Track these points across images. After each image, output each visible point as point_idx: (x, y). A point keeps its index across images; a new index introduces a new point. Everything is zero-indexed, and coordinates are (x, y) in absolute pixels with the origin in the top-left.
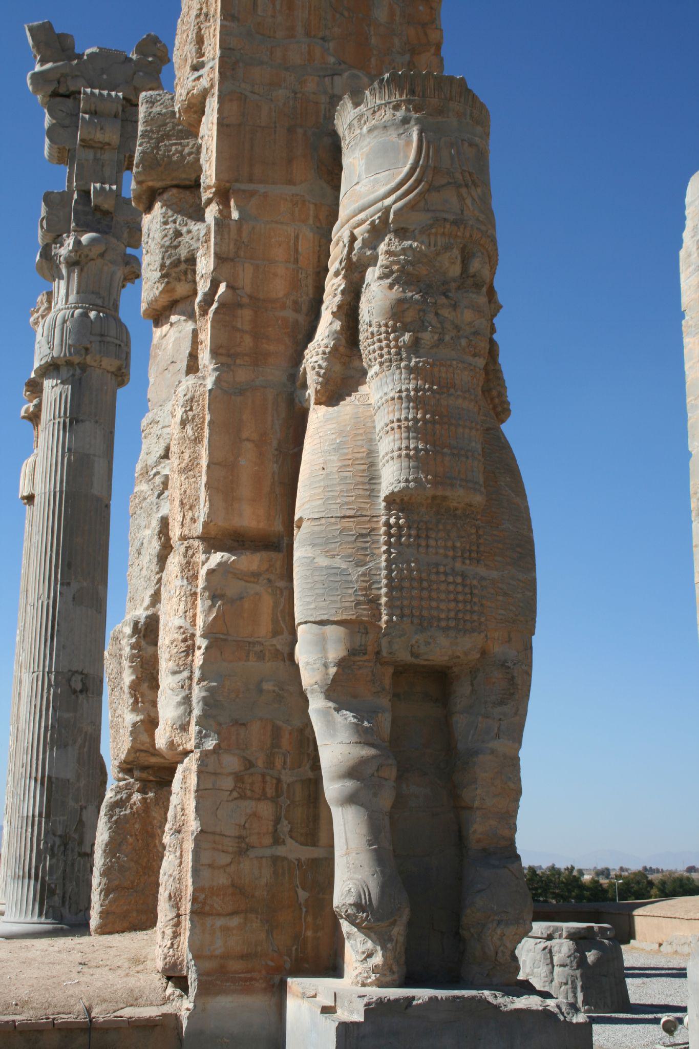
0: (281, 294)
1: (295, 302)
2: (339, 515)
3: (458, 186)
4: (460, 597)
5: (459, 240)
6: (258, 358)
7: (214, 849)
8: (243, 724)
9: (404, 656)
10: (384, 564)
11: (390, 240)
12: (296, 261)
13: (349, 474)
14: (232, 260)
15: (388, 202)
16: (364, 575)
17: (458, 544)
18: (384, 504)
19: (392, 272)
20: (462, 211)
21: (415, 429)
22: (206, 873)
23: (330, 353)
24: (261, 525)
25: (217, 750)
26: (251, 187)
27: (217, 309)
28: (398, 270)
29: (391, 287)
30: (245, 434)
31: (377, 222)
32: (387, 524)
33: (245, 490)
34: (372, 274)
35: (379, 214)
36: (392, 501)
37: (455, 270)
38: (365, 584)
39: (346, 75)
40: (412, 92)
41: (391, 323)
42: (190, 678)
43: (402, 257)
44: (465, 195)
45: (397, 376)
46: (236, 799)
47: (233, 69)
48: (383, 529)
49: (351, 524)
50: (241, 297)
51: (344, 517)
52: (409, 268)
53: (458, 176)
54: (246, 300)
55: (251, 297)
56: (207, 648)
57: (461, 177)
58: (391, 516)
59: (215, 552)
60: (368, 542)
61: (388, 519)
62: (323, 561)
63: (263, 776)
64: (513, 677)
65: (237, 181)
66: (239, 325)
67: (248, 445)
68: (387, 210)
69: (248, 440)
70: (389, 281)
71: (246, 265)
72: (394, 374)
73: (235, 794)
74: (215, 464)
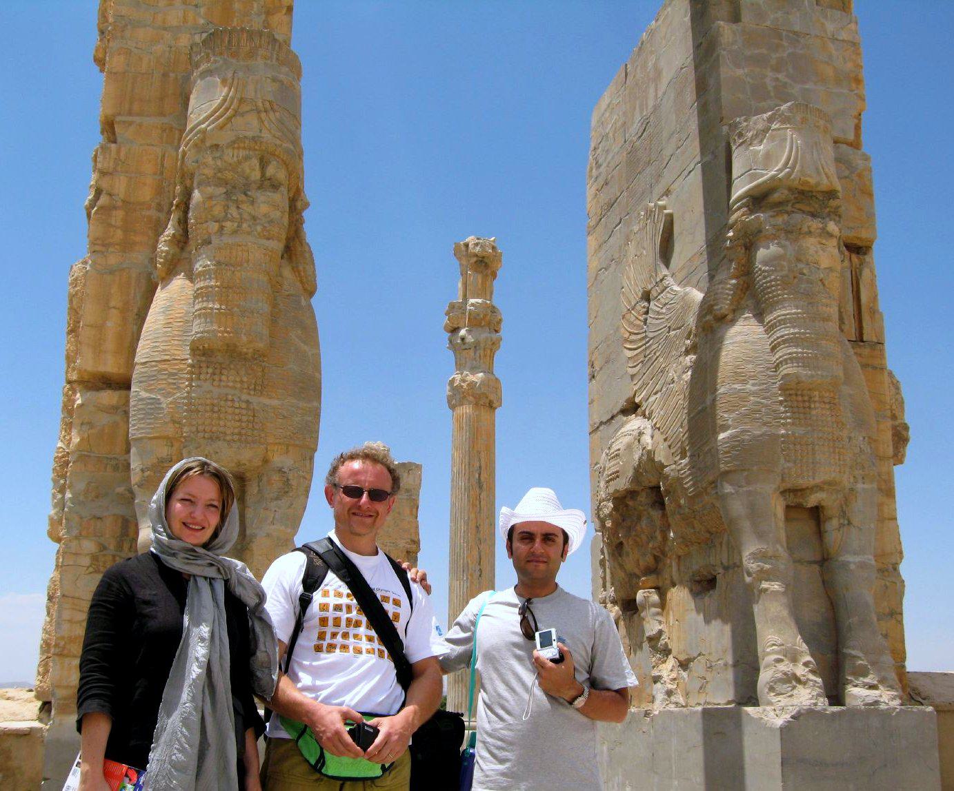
0: (148, 198)
1: (159, 204)
3: (259, 112)
4: (244, 418)
5: (257, 152)
6: (126, 246)
7: (73, 609)
8: (101, 518)
12: (162, 173)
13: (169, 329)
14: (111, 174)
17: (245, 379)
22: (66, 626)
24: (122, 371)
25: (77, 538)
26: (130, 119)
30: (112, 304)
33: (110, 345)
37: (256, 175)
44: (264, 119)
46: (91, 573)
49: (166, 366)
52: (219, 175)
53: (260, 104)
54: (119, 204)
55: (123, 201)
57: (261, 105)
63: (114, 556)
64: (288, 479)
65: (119, 114)
66: (113, 223)
67: (114, 311)
69: (114, 307)
71: (122, 178)
73: (91, 569)
74: (88, 326)
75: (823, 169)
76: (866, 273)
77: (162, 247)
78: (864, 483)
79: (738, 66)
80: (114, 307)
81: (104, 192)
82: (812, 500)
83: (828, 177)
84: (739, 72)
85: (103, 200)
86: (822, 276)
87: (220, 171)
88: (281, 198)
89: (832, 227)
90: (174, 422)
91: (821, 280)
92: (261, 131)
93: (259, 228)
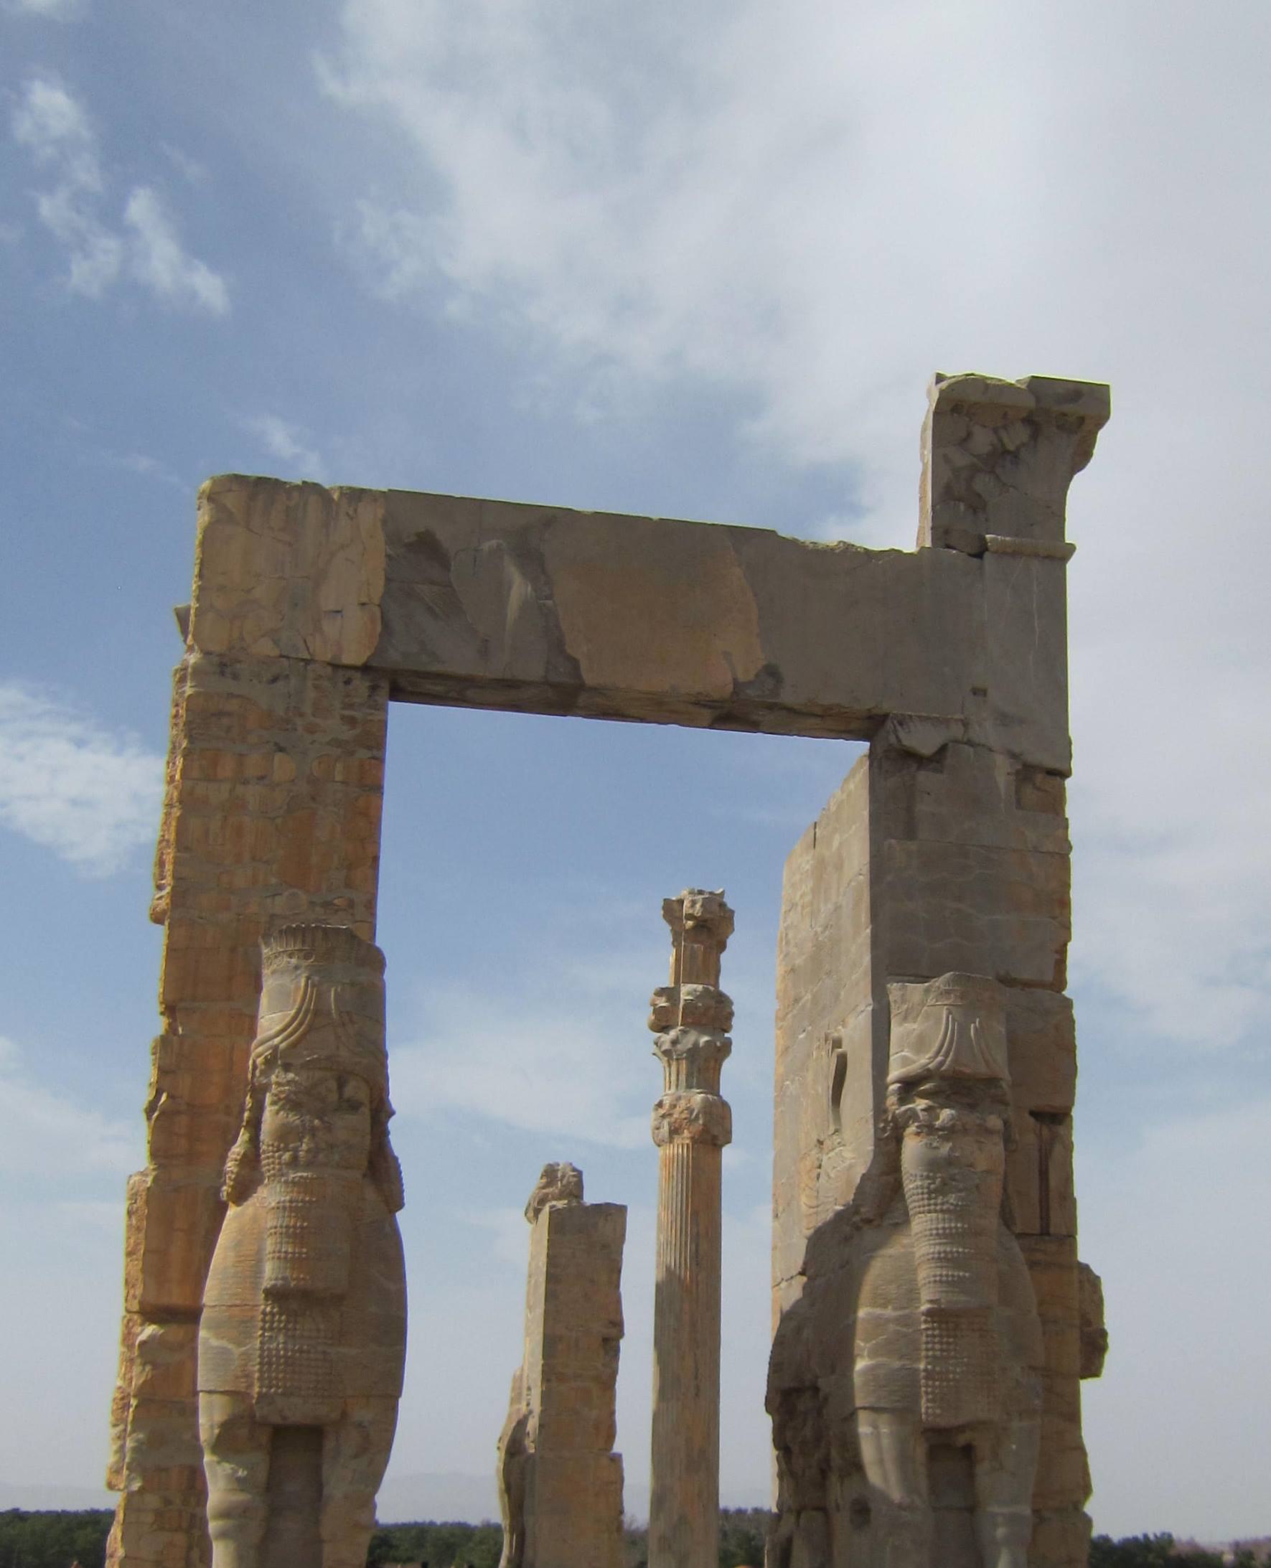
1: (228, 1107)
2: (229, 1304)
9: (276, 1419)
10: (258, 1346)
11: (279, 1072)
15: (277, 1040)
16: (243, 1354)
17: (322, 1327)
18: (263, 1295)
19: (280, 1099)
21: (288, 1236)
23: (241, 1160)
27: (158, 1116)
28: (284, 1098)
29: (277, 1112)
31: (269, 1057)
32: (264, 1313)
34: (268, 1098)
35: (270, 1052)
36: (271, 1294)
37: (334, 1097)
38: (243, 1362)
40: (304, 942)
41: (276, 1144)
42: (125, 1430)
43: (287, 1088)
45: (278, 1189)
48: (261, 1317)
51: (231, 1306)
55: (188, 1105)
56: (136, 1407)
58: (267, 1305)
59: (149, 1325)
60: (247, 1327)
61: (265, 1308)
62: (215, 1342)
68: (276, 1048)
70: (276, 1107)
72: (276, 1187)
77: (230, 1166)
83: (987, 1063)
86: (977, 1181)
88: (361, 1119)
89: (995, 1122)
91: (977, 1187)
92: (338, 1048)
93: (337, 1157)
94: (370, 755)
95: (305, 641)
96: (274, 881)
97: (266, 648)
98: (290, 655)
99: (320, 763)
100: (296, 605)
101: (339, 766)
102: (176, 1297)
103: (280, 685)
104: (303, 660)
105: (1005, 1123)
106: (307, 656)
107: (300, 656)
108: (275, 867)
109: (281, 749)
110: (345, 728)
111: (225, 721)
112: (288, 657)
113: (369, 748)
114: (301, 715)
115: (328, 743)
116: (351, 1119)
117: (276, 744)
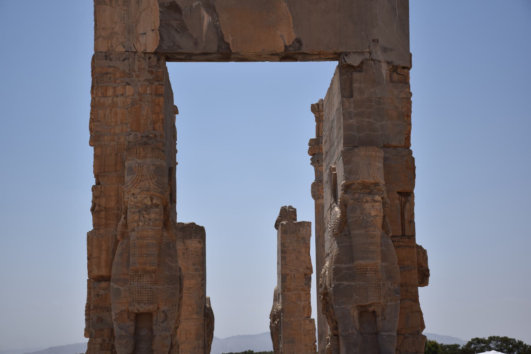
1: (118, 208)
9: (136, 311)
12: (118, 195)
14: (99, 197)
17: (149, 280)
20: (150, 187)
30: (103, 249)
39: (133, 134)
47: (99, 138)
50: (102, 208)
52: (136, 204)
55: (104, 208)
64: (167, 315)
65: (100, 173)
66: (101, 217)
69: (104, 250)
75: (372, 175)
76: (408, 205)
78: (391, 302)
79: (351, 118)
80: (104, 250)
81: (97, 205)
82: (371, 309)
84: (351, 121)
85: (97, 208)
87: (136, 203)
90: (125, 297)
91: (372, 221)
94: (159, 84)
95: (134, 45)
96: (129, 130)
97: (120, 49)
98: (129, 51)
99: (142, 88)
100: (130, 32)
101: (148, 89)
102: (104, 272)
103: (126, 61)
104: (133, 52)
105: (382, 198)
106: (135, 51)
107: (132, 51)
108: (129, 125)
109: (129, 84)
110: (150, 74)
111: (109, 76)
112: (128, 52)
113: (158, 81)
114: (134, 72)
115: (144, 81)
116: (157, 210)
117: (126, 82)
